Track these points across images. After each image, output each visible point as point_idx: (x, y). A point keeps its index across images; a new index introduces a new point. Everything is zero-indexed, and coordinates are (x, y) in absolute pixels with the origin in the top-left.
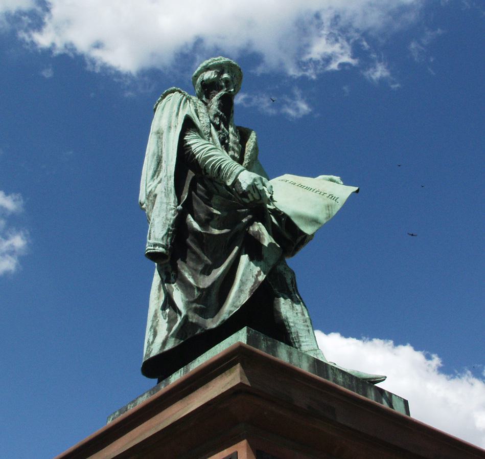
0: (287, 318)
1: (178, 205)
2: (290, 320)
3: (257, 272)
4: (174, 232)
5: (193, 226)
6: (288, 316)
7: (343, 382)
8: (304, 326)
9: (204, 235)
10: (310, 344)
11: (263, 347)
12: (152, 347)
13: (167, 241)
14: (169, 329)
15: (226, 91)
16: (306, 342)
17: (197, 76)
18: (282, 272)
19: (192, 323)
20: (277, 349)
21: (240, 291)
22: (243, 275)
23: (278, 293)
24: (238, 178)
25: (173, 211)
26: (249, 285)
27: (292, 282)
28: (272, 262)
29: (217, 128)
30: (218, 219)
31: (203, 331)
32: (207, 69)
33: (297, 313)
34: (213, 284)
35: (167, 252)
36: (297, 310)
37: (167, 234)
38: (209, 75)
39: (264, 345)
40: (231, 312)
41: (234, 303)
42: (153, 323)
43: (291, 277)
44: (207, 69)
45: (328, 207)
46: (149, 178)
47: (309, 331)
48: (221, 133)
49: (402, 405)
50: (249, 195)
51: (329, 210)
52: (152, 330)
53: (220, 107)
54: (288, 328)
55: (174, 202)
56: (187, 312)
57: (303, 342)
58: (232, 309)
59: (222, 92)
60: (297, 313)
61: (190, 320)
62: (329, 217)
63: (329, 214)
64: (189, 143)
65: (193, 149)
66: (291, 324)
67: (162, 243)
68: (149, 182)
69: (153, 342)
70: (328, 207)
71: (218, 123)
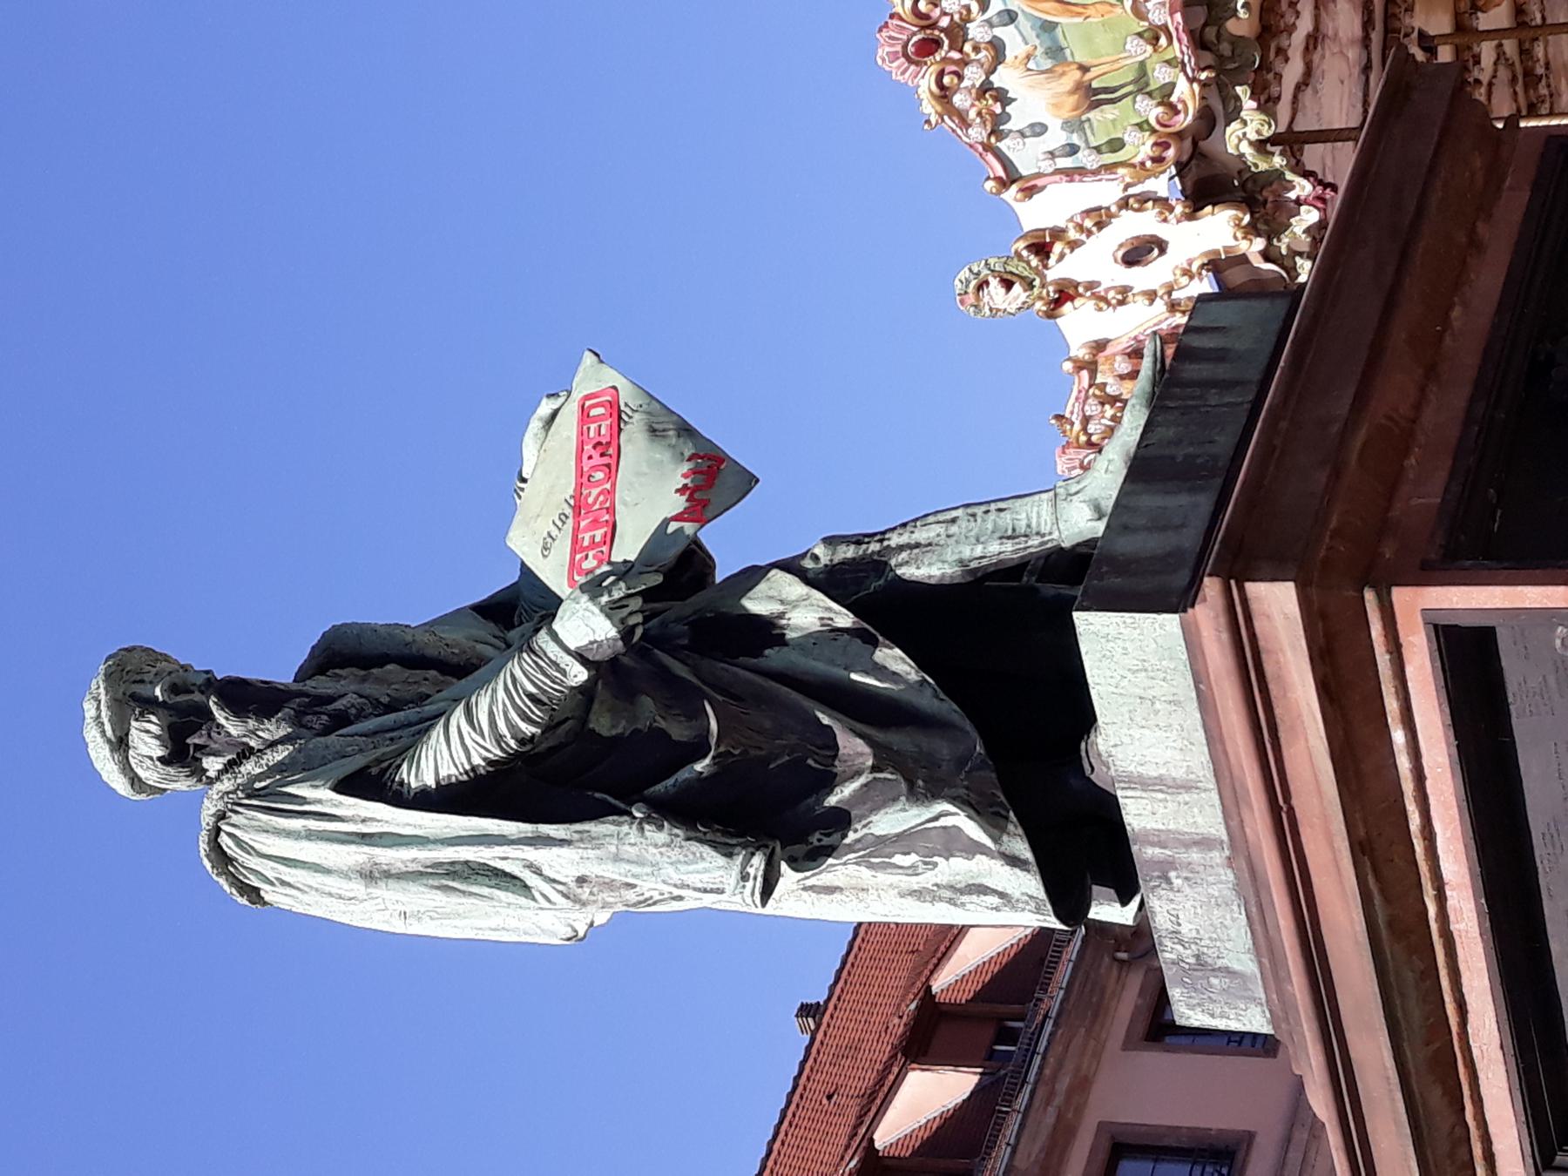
1: (630, 814)
9: (722, 749)
12: (1016, 894)
14: (973, 849)
17: (135, 781)
22: (832, 662)
24: (572, 648)
29: (341, 720)
32: (121, 744)
38: (147, 741)
42: (941, 899)
44: (121, 744)
46: (523, 901)
47: (1000, 510)
50: (632, 621)
52: (965, 899)
54: (985, 562)
55: (620, 824)
57: (1029, 526)
64: (431, 782)
65: (453, 771)
68: (534, 899)
69: (1002, 895)
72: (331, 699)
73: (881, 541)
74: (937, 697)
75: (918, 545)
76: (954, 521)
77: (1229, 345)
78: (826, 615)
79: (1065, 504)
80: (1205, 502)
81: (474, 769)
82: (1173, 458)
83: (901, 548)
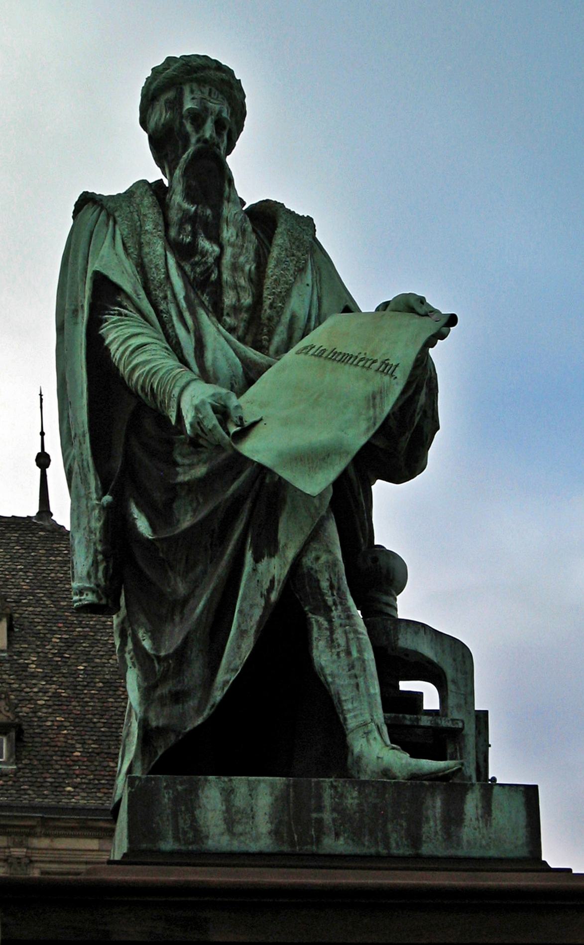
0: (322, 668)
1: (104, 494)
2: (327, 671)
3: (268, 583)
5: (134, 526)
6: (323, 663)
7: (359, 805)
8: (350, 677)
10: (358, 712)
11: (166, 800)
16: (354, 709)
18: (312, 569)
20: (197, 796)
22: (244, 598)
23: (310, 615)
26: (257, 613)
27: (332, 587)
28: (291, 554)
29: (185, 252)
30: (189, 491)
33: (338, 654)
36: (339, 646)
39: (167, 796)
41: (229, 663)
43: (327, 576)
47: (357, 686)
48: (197, 264)
49: (519, 800)
53: (189, 196)
57: (349, 711)
58: (227, 677)
60: (338, 654)
61: (154, 724)
66: (330, 679)
72: (216, 238)
73: (335, 604)
75: (332, 631)
76: (349, 653)
77: (467, 822)
78: (276, 584)
79: (361, 733)
80: (265, 844)
81: (118, 370)
82: (320, 808)
83: (330, 621)
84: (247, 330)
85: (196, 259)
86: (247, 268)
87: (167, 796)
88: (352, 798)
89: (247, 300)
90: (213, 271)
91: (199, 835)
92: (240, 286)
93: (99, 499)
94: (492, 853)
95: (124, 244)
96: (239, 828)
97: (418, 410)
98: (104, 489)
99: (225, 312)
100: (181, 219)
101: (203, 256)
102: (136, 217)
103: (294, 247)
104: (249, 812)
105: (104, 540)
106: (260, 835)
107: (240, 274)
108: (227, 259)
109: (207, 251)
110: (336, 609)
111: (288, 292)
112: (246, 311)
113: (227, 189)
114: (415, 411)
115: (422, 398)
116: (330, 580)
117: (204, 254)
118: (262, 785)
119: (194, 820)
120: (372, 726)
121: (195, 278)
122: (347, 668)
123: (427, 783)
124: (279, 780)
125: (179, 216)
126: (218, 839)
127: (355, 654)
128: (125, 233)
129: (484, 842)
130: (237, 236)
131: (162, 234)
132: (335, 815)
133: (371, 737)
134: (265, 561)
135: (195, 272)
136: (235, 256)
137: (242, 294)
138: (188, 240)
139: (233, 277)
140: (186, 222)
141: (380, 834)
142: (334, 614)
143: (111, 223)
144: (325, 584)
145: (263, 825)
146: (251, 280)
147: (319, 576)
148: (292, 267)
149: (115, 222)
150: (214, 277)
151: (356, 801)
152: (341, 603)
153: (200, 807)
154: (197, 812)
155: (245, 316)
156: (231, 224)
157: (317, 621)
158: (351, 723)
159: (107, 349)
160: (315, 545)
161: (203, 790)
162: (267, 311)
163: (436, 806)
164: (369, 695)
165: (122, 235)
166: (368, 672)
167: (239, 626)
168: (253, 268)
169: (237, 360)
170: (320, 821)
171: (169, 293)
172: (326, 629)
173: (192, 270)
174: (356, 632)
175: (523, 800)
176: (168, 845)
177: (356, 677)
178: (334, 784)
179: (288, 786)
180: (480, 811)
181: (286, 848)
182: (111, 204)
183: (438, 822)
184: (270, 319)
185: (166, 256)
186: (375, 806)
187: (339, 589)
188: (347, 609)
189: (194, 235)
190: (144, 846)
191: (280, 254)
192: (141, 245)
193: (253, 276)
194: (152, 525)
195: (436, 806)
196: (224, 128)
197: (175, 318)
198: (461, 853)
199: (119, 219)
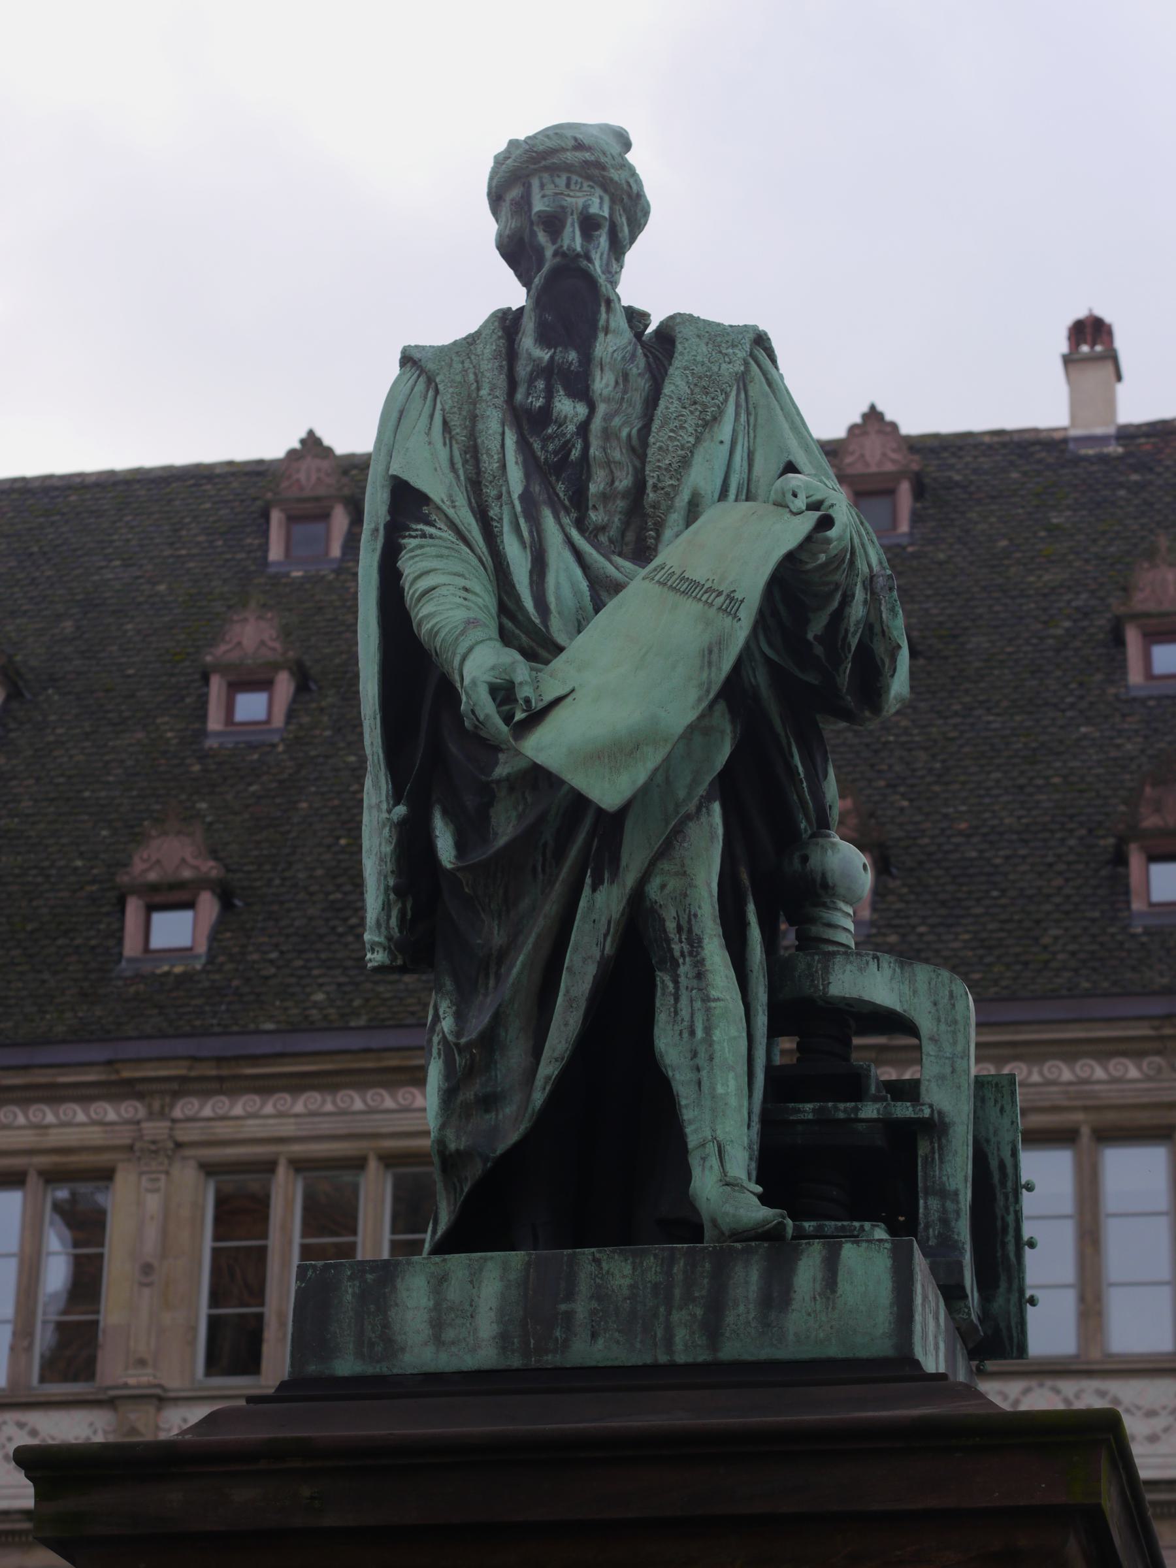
0: (662, 1056)
4: (400, 891)
7: (631, 1287)
9: (459, 875)
11: (349, 1297)
13: (388, 927)
15: (555, 254)
19: (458, 1151)
21: (571, 1001)
25: (386, 830)
27: (679, 929)
28: (630, 878)
29: (530, 422)
30: (512, 789)
31: (489, 1165)
33: (681, 1034)
34: (497, 1019)
35: (394, 959)
37: (386, 907)
40: (548, 1078)
45: (709, 654)
47: (699, 1083)
48: (550, 438)
51: (710, 663)
56: (443, 1127)
59: (545, 270)
60: (681, 1034)
62: (708, 691)
63: (710, 683)
66: (670, 1074)
67: (377, 939)
70: (710, 652)
71: (539, 403)
72: (581, 390)
73: (682, 955)
74: (546, 1083)
75: (677, 999)
76: (692, 1033)
82: (570, 1296)
83: (676, 983)
84: (626, 525)
85: (550, 431)
86: (624, 433)
87: (350, 1290)
88: (624, 1277)
89: (624, 481)
90: (573, 446)
91: (390, 1345)
92: (615, 462)
93: (389, 811)
94: (833, 1351)
95: (445, 423)
96: (449, 1334)
97: (852, 630)
98: (397, 797)
99: (590, 505)
100: (531, 374)
101: (560, 426)
102: (471, 377)
103: (697, 390)
104: (467, 1307)
105: (399, 871)
106: (480, 1343)
107: (615, 443)
108: (596, 425)
109: (566, 417)
110: (684, 964)
111: (685, 462)
112: (623, 497)
113: (604, 316)
114: (847, 631)
115: (857, 611)
116: (677, 919)
117: (561, 424)
118: (490, 1265)
119: (386, 1325)
120: (712, 1149)
121: (546, 459)
122: (689, 1055)
123: (738, 1245)
124: (517, 1258)
125: (529, 369)
126: (419, 1352)
127: (700, 1033)
128: (447, 407)
129: (822, 1335)
130: (617, 383)
131: (500, 401)
132: (594, 1304)
133: (707, 1164)
134: (603, 889)
135: (547, 451)
136: (608, 418)
137: (617, 473)
138: (538, 404)
139: (604, 449)
140: (537, 377)
141: (660, 1333)
142: (682, 970)
143: (431, 393)
144: (671, 926)
145: (486, 1326)
146: (633, 449)
147: (664, 914)
148: (691, 422)
149: (437, 392)
150: (575, 454)
151: (627, 1282)
152: (691, 954)
153: (397, 1305)
154: (392, 1313)
155: (621, 504)
156: (606, 369)
157: (663, 982)
158: (692, 1141)
159: (403, 589)
160: (665, 865)
161: (403, 1279)
162: (651, 496)
163: (748, 1280)
164: (713, 1097)
165: (443, 410)
166: (717, 1060)
167: (567, 991)
168: (634, 431)
169: (584, 585)
170: (569, 1316)
171: (504, 489)
172: (671, 994)
173: (542, 448)
174: (706, 999)
175: (889, 1263)
176: (346, 1366)
177: (698, 1069)
178: (597, 1255)
179: (528, 1264)
180: (818, 1288)
181: (516, 1362)
182: (431, 366)
183: (751, 1306)
184: (655, 506)
185: (503, 434)
186: (656, 1286)
187: (690, 931)
188: (699, 963)
189: (549, 395)
190: (312, 1368)
191: (667, 408)
192: (474, 418)
193: (635, 442)
194: (461, 847)
195: (748, 1280)
196: (598, 226)
197: (506, 528)
198: (781, 1354)
199: (441, 387)
